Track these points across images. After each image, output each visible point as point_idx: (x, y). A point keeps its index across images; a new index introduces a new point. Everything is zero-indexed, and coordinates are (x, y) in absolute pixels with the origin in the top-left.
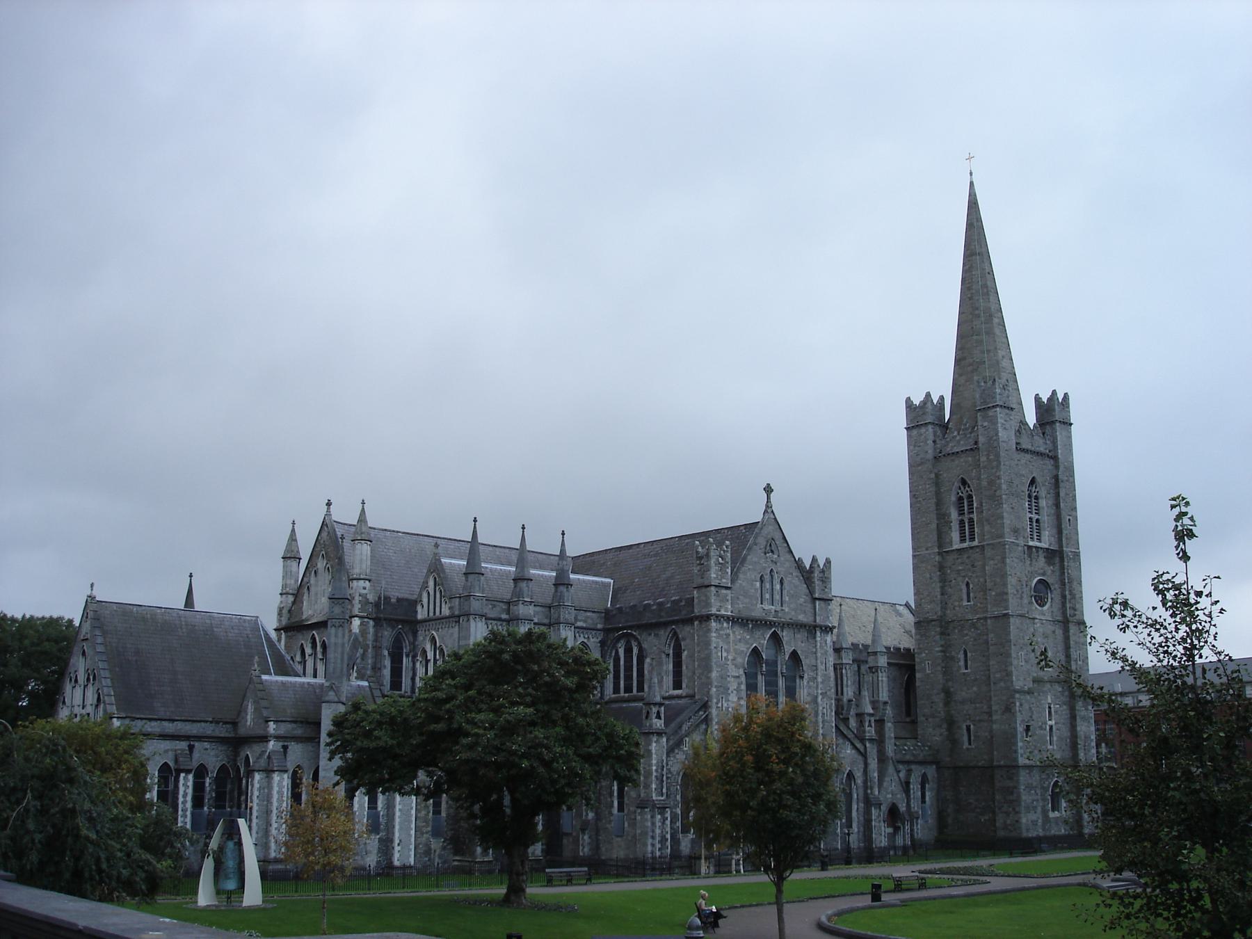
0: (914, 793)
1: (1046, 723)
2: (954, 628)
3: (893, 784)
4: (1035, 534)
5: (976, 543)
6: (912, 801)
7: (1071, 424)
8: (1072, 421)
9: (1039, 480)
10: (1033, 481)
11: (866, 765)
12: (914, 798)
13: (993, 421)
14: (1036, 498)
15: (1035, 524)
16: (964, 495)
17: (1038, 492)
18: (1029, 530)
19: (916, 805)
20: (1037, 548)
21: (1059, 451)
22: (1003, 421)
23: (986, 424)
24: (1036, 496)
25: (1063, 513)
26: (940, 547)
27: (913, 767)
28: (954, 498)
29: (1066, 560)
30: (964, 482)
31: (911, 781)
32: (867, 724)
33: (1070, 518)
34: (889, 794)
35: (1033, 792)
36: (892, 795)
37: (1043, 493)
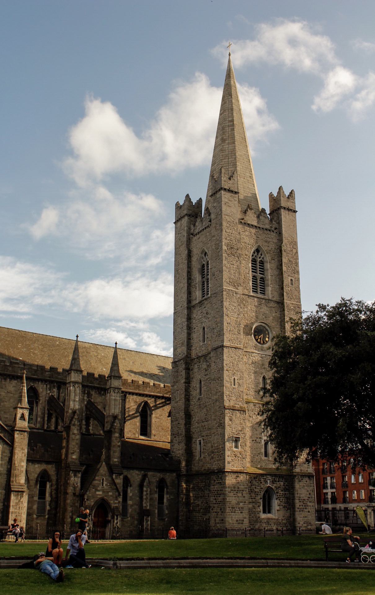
0: (147, 494)
1: (260, 438)
2: (195, 364)
3: (105, 483)
4: (259, 289)
5: (209, 295)
6: (144, 501)
7: (295, 212)
8: (296, 210)
9: (264, 249)
10: (257, 251)
11: (12, 453)
12: (146, 499)
13: (219, 201)
14: (262, 263)
15: (259, 282)
16: (205, 263)
17: (263, 258)
18: (251, 284)
19: (148, 504)
20: (258, 298)
21: (283, 229)
22: (227, 200)
23: (215, 205)
24: (261, 261)
25: (285, 275)
26: (189, 301)
27: (150, 473)
28: (200, 267)
29: (286, 309)
30: (206, 254)
31: (145, 484)
32: (19, 416)
33: (293, 279)
34: (99, 491)
35: (240, 495)
36: (103, 492)
37: (268, 258)
